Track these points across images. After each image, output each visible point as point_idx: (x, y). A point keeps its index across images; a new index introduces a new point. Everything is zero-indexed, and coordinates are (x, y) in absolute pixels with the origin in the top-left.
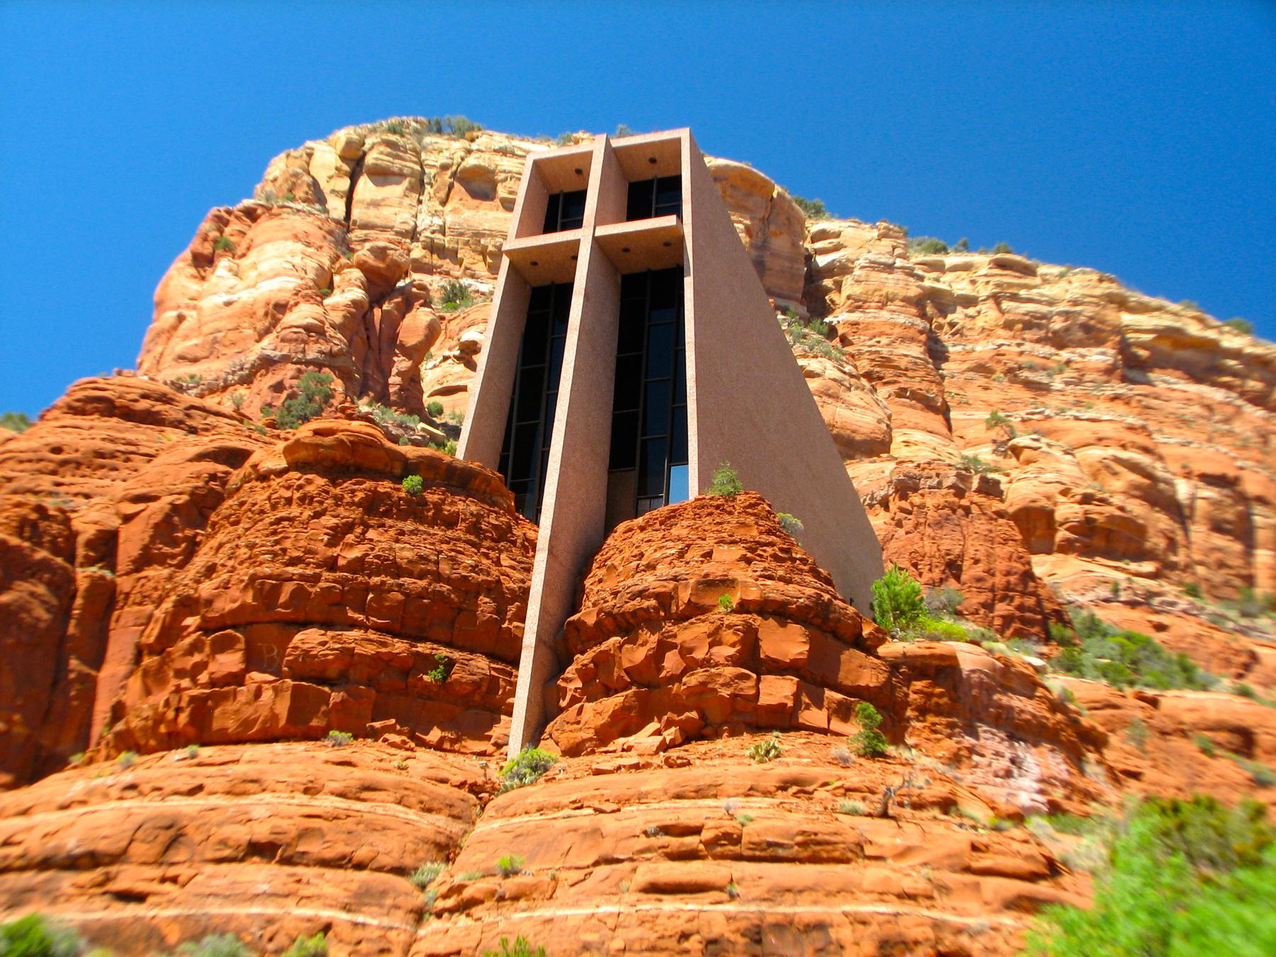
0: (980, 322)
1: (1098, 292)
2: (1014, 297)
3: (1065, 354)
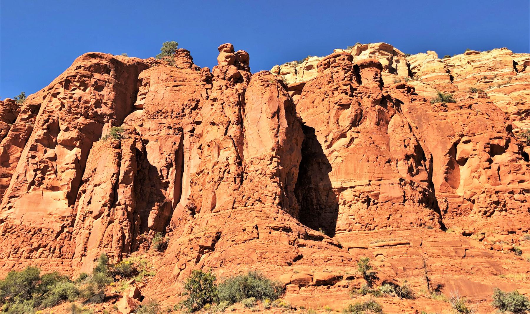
0: (465, 71)
1: (502, 53)
2: (473, 61)
3: (495, 73)
